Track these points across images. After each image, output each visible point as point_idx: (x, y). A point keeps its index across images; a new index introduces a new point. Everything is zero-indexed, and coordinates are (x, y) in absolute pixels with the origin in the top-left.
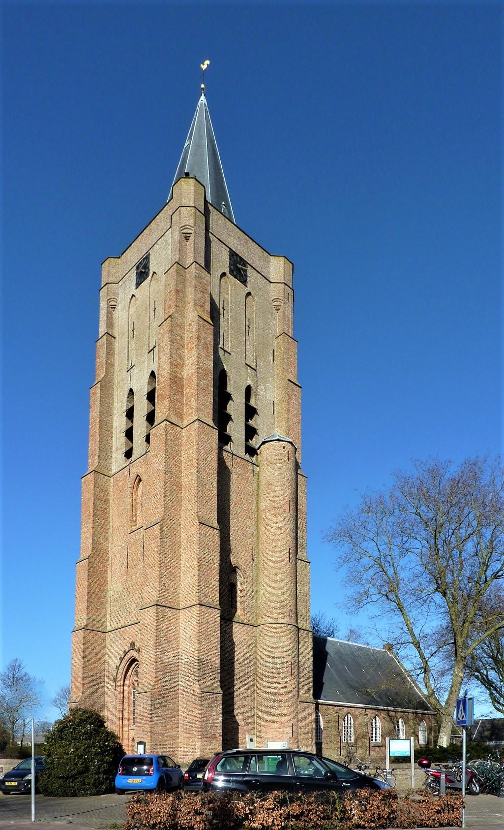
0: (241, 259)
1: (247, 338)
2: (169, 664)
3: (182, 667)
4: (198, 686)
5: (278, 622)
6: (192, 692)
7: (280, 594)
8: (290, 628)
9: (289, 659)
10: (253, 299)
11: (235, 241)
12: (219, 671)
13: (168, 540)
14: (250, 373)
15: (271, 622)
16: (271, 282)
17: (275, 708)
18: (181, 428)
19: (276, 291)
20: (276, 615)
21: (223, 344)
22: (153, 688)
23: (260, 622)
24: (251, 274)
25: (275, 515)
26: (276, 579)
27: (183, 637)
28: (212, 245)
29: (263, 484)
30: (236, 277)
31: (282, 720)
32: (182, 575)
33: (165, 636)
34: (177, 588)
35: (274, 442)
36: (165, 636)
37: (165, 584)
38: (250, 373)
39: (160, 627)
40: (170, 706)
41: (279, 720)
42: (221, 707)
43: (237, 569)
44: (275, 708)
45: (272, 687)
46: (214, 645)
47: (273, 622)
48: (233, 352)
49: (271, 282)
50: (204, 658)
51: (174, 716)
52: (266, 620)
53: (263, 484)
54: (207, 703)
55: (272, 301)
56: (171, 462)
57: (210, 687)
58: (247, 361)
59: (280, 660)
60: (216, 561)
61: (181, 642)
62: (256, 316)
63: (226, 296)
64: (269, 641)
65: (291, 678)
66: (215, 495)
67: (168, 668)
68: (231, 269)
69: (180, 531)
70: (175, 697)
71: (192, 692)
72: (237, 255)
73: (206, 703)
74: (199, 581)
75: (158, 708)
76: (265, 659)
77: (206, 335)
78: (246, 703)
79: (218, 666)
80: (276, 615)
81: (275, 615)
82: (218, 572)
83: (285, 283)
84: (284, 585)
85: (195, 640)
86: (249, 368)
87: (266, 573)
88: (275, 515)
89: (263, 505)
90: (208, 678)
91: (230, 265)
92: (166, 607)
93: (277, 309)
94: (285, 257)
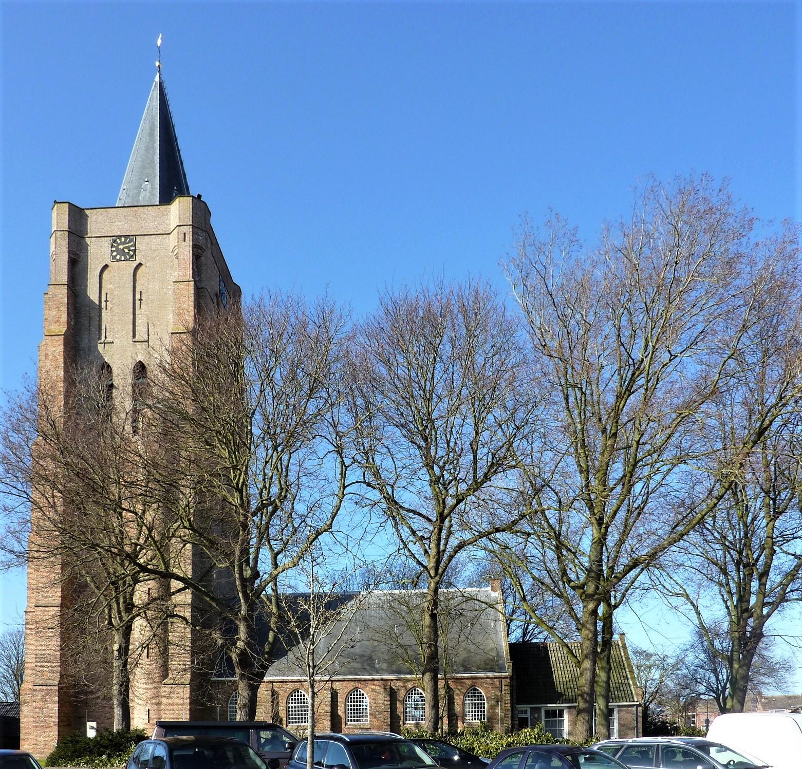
0: (126, 237)
1: (137, 312)
11: (120, 223)
14: (140, 348)
16: (169, 234)
19: (173, 240)
21: (106, 337)
24: (141, 243)
28: (89, 248)
30: (120, 260)
38: (140, 348)
42: (57, 698)
48: (117, 338)
49: (169, 234)
54: (40, 695)
58: (137, 338)
63: (110, 286)
68: (113, 256)
72: (120, 237)
77: (54, 349)
83: (178, 226)
86: (138, 343)
91: (112, 252)
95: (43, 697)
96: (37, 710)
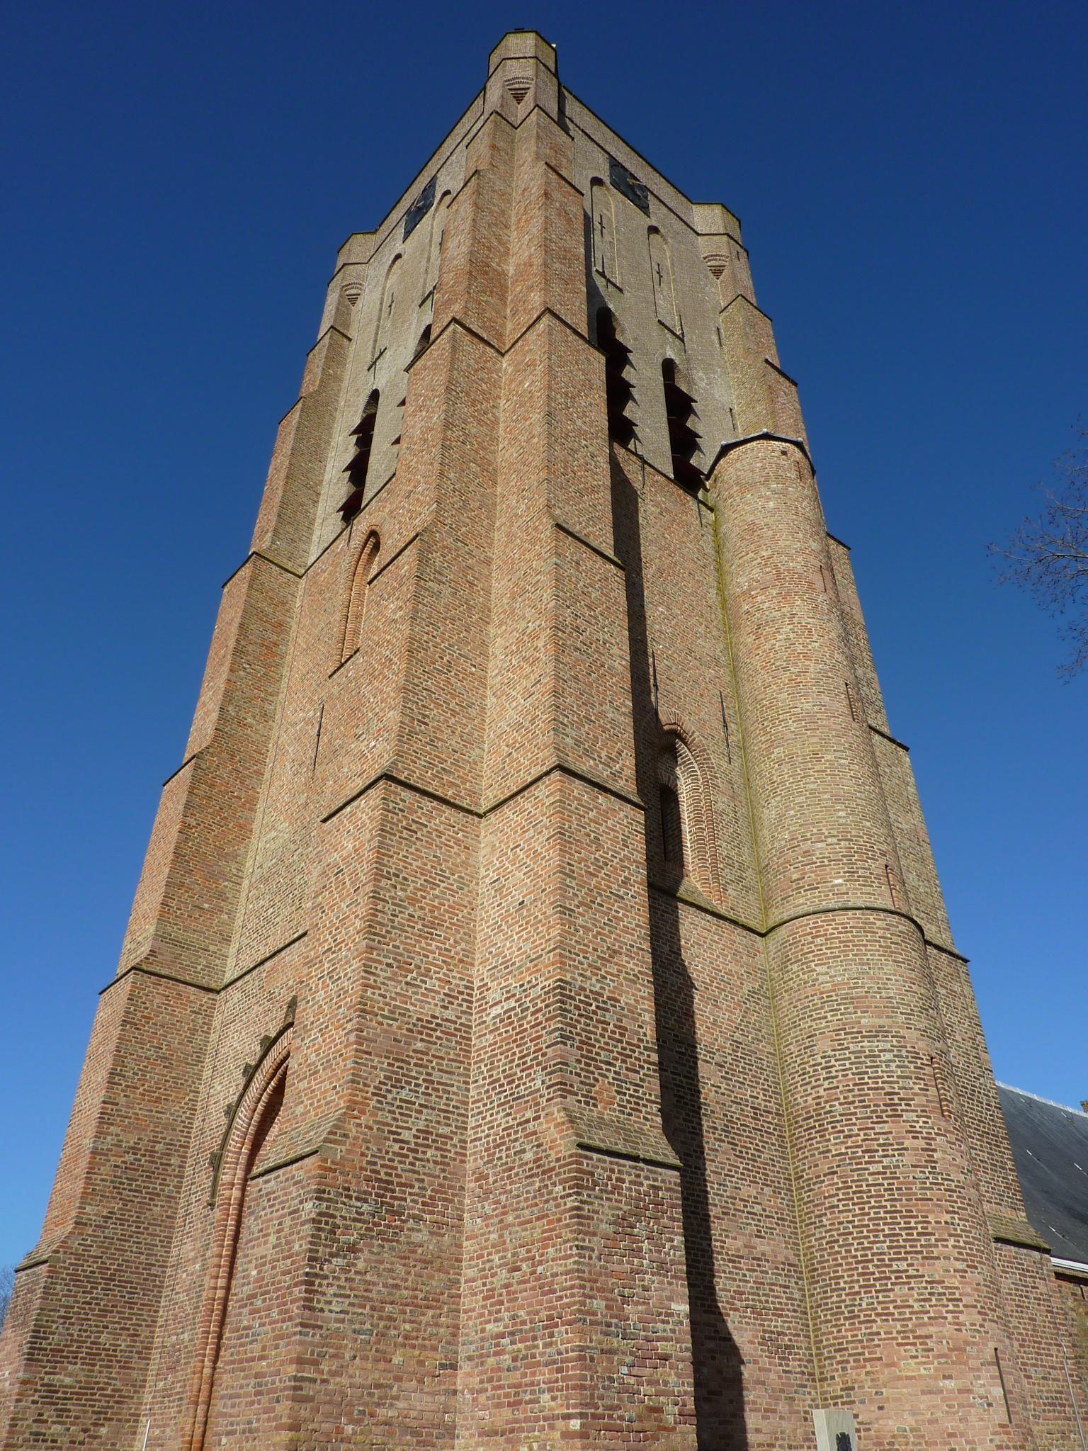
2: (426, 1026)
3: (481, 1042)
4: (560, 1117)
5: (850, 904)
6: (529, 1156)
7: (841, 814)
8: (901, 928)
9: (921, 1044)
10: (665, 240)
12: (655, 1057)
13: (447, 591)
15: (824, 905)
16: (698, 234)
17: (904, 1265)
18: (498, 351)
20: (840, 881)
22: (337, 1133)
23: (776, 916)
25: (785, 597)
26: (817, 768)
27: (489, 911)
29: (733, 535)
31: (949, 1330)
32: (491, 701)
33: (413, 901)
34: (472, 740)
35: (754, 444)
36: (413, 901)
37: (425, 716)
39: (393, 864)
40: (417, 1237)
41: (932, 1330)
42: (679, 1240)
43: (679, 743)
44: (903, 1265)
45: (873, 1168)
46: (628, 939)
47: (831, 906)
49: (698, 234)
50: (587, 986)
51: (433, 1302)
52: (803, 902)
53: (733, 535)
55: (705, 258)
56: (464, 409)
57: (620, 1128)
59: (888, 1046)
60: (615, 650)
61: (480, 936)
62: (672, 264)
64: (827, 975)
65: (943, 1124)
66: (605, 489)
67: (419, 1045)
69: (489, 577)
70: (446, 1193)
71: (529, 1156)
73: (605, 1213)
74: (556, 693)
75: (353, 1249)
76: (823, 1045)
78: (767, 1249)
79: (650, 1032)
80: (840, 881)
81: (836, 882)
82: (627, 686)
83: (728, 235)
84: (848, 785)
85: (545, 909)
87: (777, 753)
88: (785, 597)
89: (741, 581)
90: (606, 1087)
92: (425, 793)
93: (717, 272)
94: (723, 206)
95: (623, 1223)
96: (598, 1304)
